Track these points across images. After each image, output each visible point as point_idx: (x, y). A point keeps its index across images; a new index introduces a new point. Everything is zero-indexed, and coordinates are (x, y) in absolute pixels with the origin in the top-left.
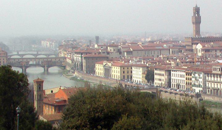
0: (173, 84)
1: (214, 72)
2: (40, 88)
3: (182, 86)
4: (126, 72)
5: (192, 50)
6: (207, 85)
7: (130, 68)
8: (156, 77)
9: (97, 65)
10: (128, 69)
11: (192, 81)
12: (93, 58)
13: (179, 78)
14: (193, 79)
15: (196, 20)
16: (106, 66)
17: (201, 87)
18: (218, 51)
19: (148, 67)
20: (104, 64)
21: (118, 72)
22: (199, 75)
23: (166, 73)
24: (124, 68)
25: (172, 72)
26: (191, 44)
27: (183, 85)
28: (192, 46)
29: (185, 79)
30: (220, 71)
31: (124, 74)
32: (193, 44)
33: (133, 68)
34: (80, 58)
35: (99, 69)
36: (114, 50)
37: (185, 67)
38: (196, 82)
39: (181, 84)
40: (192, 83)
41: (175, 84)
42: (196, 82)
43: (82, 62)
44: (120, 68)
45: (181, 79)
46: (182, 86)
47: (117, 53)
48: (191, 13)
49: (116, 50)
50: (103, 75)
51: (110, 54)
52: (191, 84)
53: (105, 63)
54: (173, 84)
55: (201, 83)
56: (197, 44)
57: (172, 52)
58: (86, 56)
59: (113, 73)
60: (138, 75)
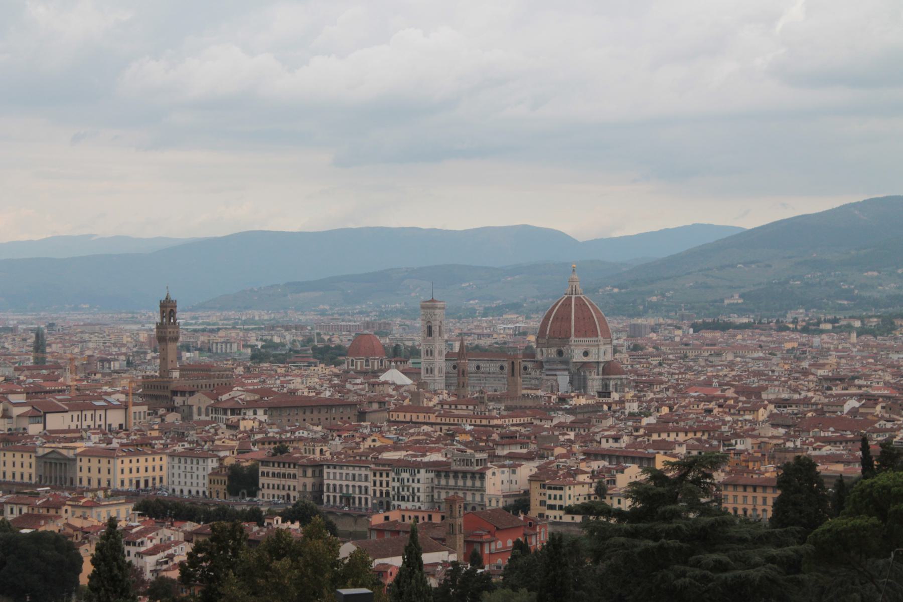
0: (328, 497)
1: (454, 467)
3: (360, 499)
4: (127, 471)
6: (436, 496)
8: (262, 480)
11: (390, 489)
13: (351, 483)
14: (392, 484)
18: (260, 412)
19: (221, 459)
22: (411, 475)
23: (305, 472)
24: (122, 462)
25: (326, 470)
26: (169, 395)
29: (370, 485)
32: (175, 393)
38: (403, 490)
39: (357, 496)
40: (392, 493)
41: (338, 495)
42: (403, 490)
45: (357, 484)
46: (360, 499)
52: (388, 493)
54: (328, 497)
56: (192, 393)
59: (84, 475)
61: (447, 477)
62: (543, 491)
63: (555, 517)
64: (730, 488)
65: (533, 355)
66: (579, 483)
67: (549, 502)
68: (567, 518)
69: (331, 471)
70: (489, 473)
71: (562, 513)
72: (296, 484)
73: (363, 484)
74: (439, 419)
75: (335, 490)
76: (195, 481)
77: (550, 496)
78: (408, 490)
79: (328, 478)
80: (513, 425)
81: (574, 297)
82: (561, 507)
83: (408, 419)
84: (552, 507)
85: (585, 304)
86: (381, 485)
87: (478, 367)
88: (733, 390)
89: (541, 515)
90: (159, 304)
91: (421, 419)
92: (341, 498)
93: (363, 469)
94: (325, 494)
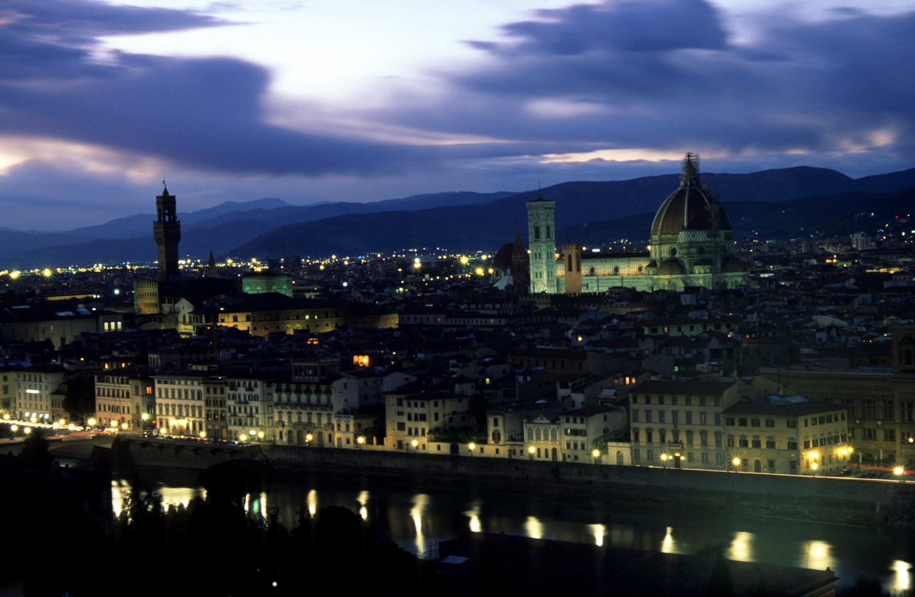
8: (99, 401)
17: (257, 425)
19: (68, 372)
23: (137, 388)
25: (157, 386)
29: (202, 403)
30: (315, 374)
37: (200, 368)
38: (240, 411)
42: (240, 411)
55: (257, 412)
61: (288, 391)
62: (400, 409)
64: (641, 399)
65: (647, 254)
66: (452, 396)
69: (163, 386)
70: (337, 385)
71: (424, 440)
72: (129, 404)
74: (449, 320)
78: (245, 409)
79: (160, 396)
80: (527, 325)
83: (418, 322)
87: (592, 270)
88: (852, 281)
89: (400, 444)
90: (155, 201)
91: (431, 322)
93: (196, 383)
94: (158, 418)
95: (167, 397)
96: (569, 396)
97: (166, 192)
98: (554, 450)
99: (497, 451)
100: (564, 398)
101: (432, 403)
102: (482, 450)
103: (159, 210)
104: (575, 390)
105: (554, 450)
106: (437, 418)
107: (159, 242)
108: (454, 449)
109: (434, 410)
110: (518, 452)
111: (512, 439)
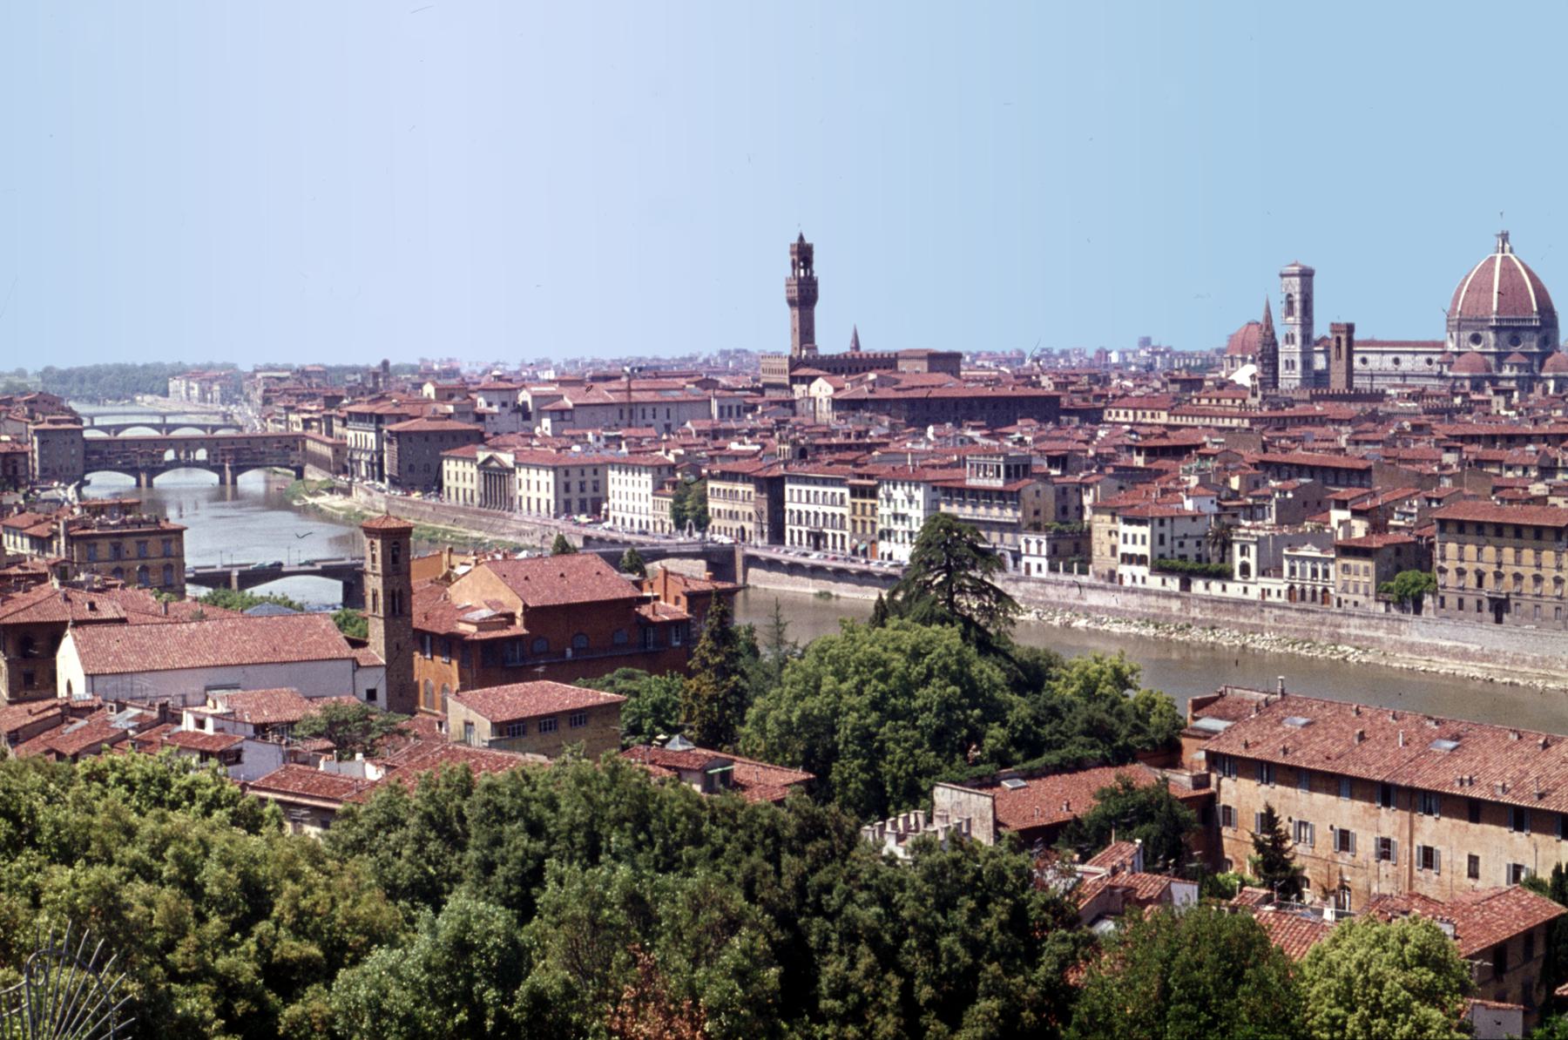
0: (792, 532)
2: (395, 559)
3: (834, 536)
4: (575, 487)
5: (791, 404)
7: (589, 472)
8: (713, 505)
9: (452, 463)
10: (583, 474)
12: (425, 435)
15: (801, 291)
16: (494, 464)
20: (482, 456)
21: (543, 487)
24: (567, 473)
25: (788, 487)
26: (785, 380)
27: (838, 533)
28: (792, 391)
29: (846, 511)
31: (567, 496)
32: (794, 380)
33: (613, 475)
34: (372, 436)
35: (460, 475)
36: (504, 405)
39: (829, 531)
41: (804, 529)
43: (380, 451)
44: (551, 473)
46: (834, 536)
47: (514, 417)
48: (783, 268)
49: (510, 406)
50: (477, 499)
51: (488, 419)
53: (487, 454)
54: (792, 532)
56: (813, 379)
57: (721, 408)
58: (395, 427)
59: (522, 492)
60: (633, 501)
63: (1134, 578)
67: (1123, 548)
68: (1155, 582)
69: (796, 487)
71: (1142, 571)
73: (838, 510)
75: (800, 522)
76: (637, 504)
77: (1125, 536)
79: (791, 501)
81: (1499, 256)
82: (1141, 560)
83: (1131, 419)
84: (1128, 559)
85: (1516, 269)
86: (864, 513)
90: (788, 249)
91: (1149, 420)
92: (809, 534)
94: (788, 528)
95: (800, 501)
96: (1347, 522)
97: (801, 238)
98: (1325, 591)
99: (1245, 590)
100: (1340, 523)
101: (1156, 522)
102: (1224, 588)
103: (794, 264)
104: (1356, 514)
105: (1325, 591)
106: (1162, 542)
107: (791, 303)
108: (1186, 585)
109: (1159, 530)
110: (1274, 593)
111: (1262, 573)
